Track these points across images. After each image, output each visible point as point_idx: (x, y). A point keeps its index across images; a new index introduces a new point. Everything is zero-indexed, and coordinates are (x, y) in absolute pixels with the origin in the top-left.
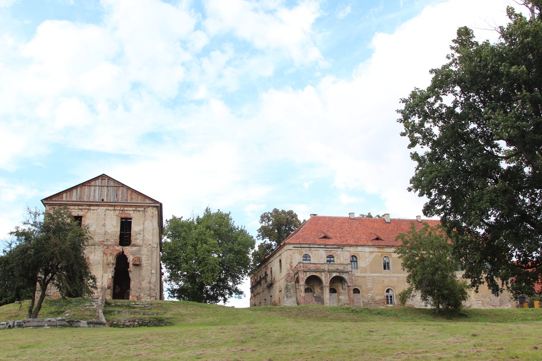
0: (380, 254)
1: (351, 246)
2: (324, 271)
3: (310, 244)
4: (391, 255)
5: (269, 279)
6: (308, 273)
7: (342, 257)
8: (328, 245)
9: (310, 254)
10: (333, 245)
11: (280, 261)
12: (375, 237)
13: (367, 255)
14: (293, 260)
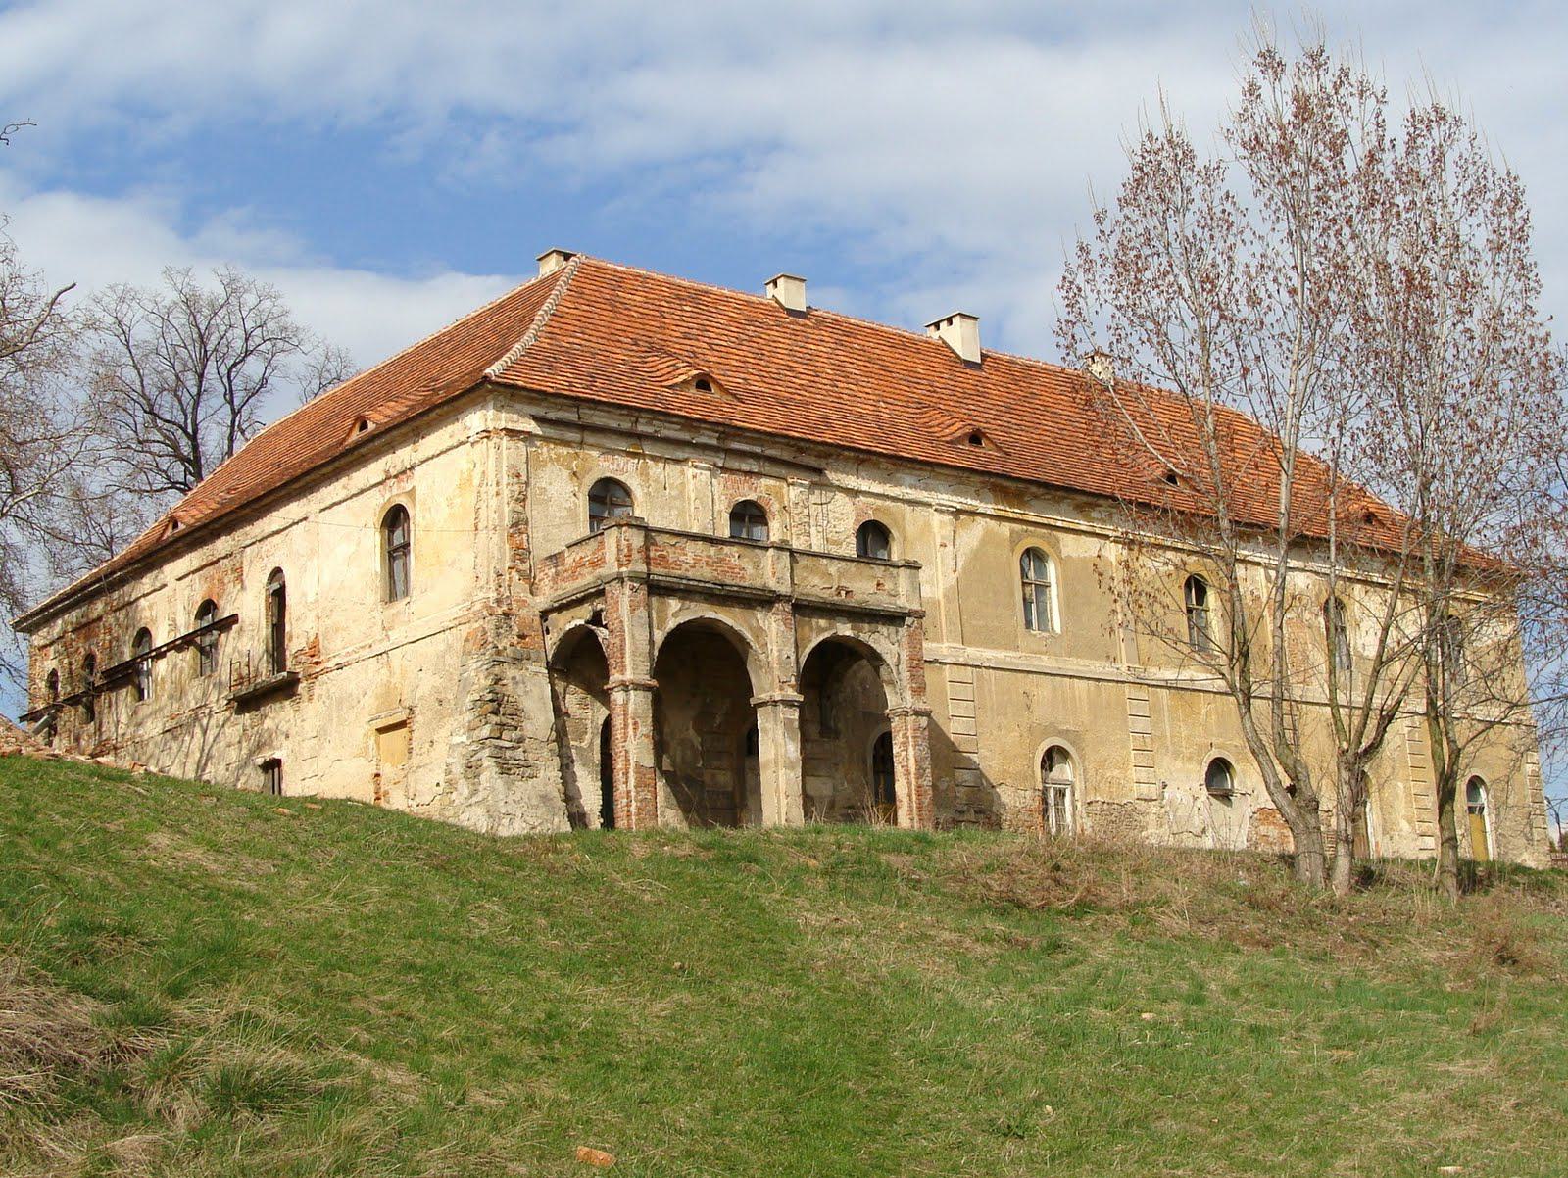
0: (1006, 529)
1: (863, 459)
2: (764, 600)
3: (634, 412)
4: (1056, 545)
5: (244, 647)
6: (674, 604)
7: (818, 518)
8: (739, 433)
9: (633, 482)
10: (772, 438)
11: (395, 518)
12: (958, 429)
13: (940, 523)
14: (533, 512)
